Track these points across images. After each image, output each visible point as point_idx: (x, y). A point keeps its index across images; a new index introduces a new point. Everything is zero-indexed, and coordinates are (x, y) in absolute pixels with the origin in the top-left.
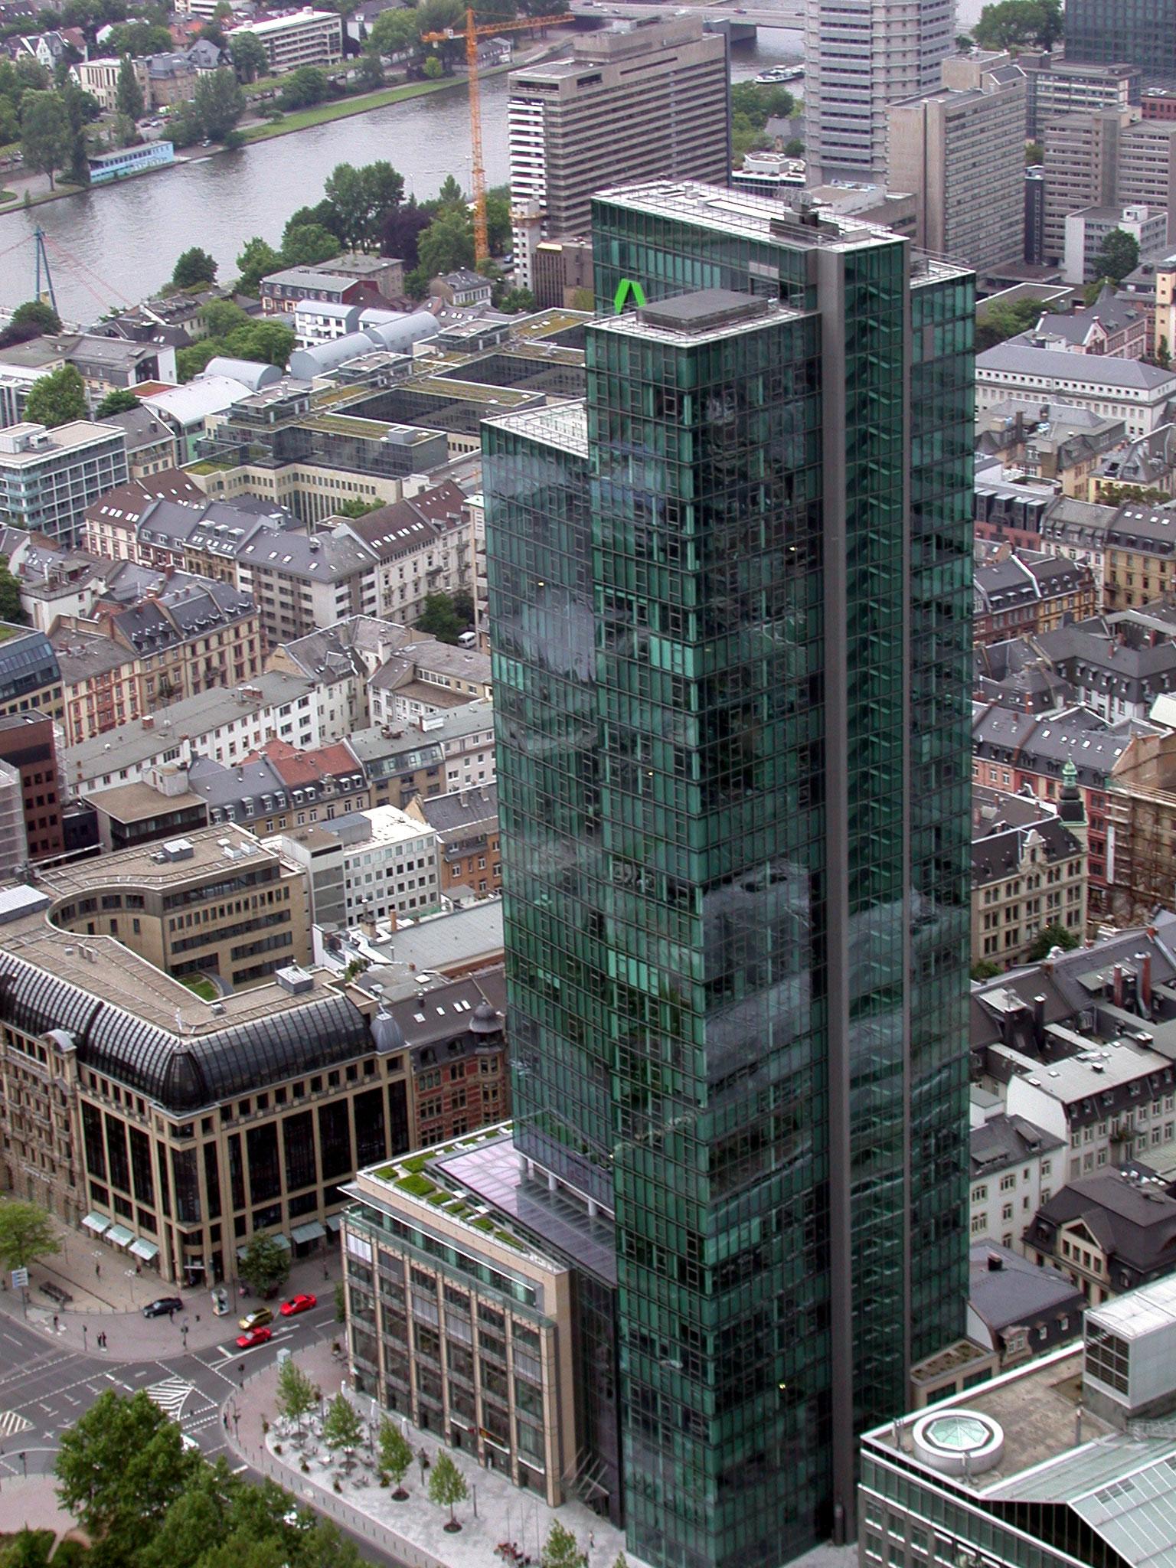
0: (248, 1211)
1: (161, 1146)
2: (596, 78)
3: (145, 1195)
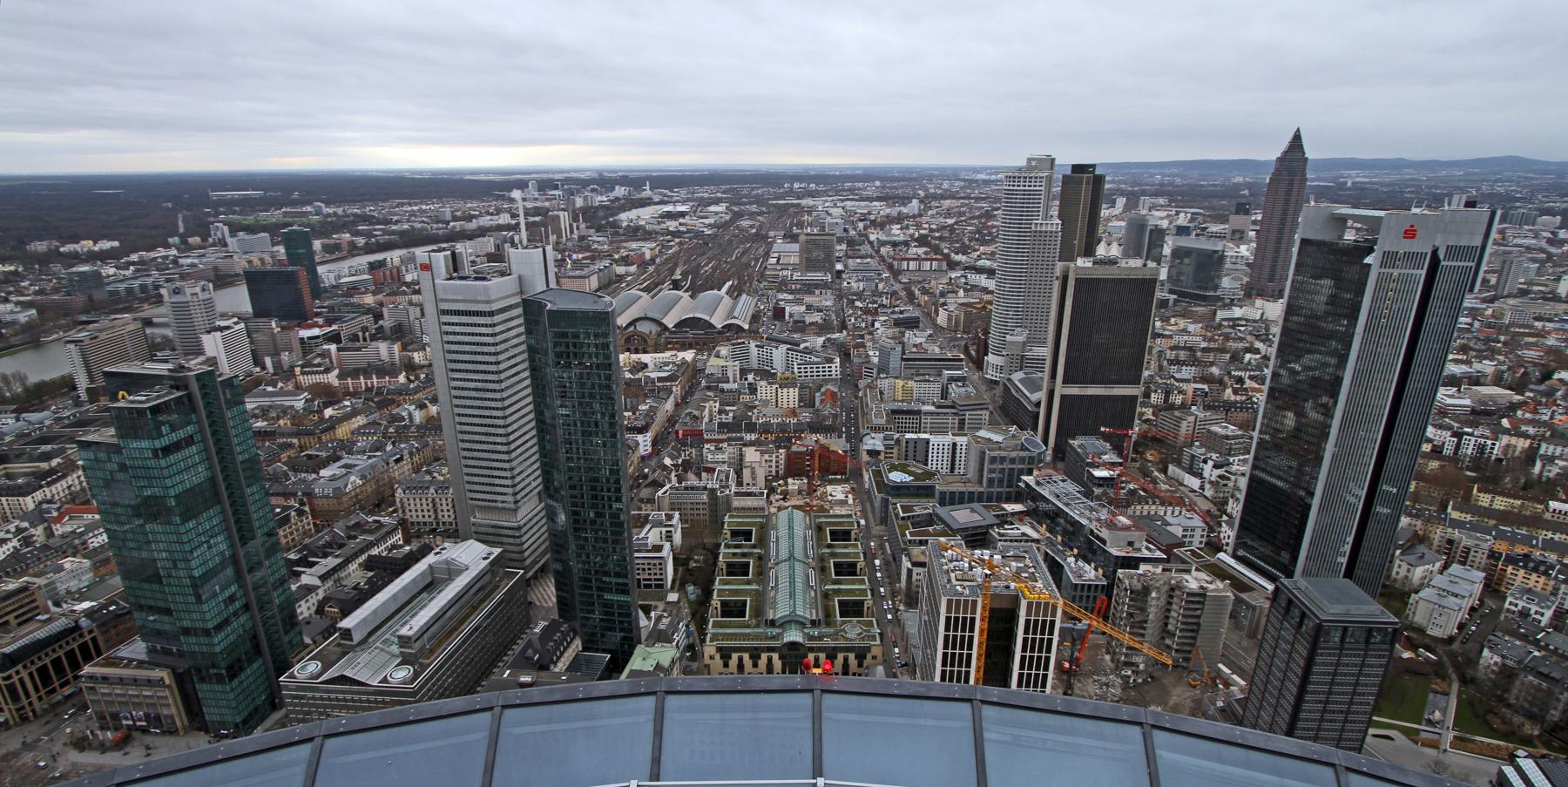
0: (42, 692)
2: (96, 338)
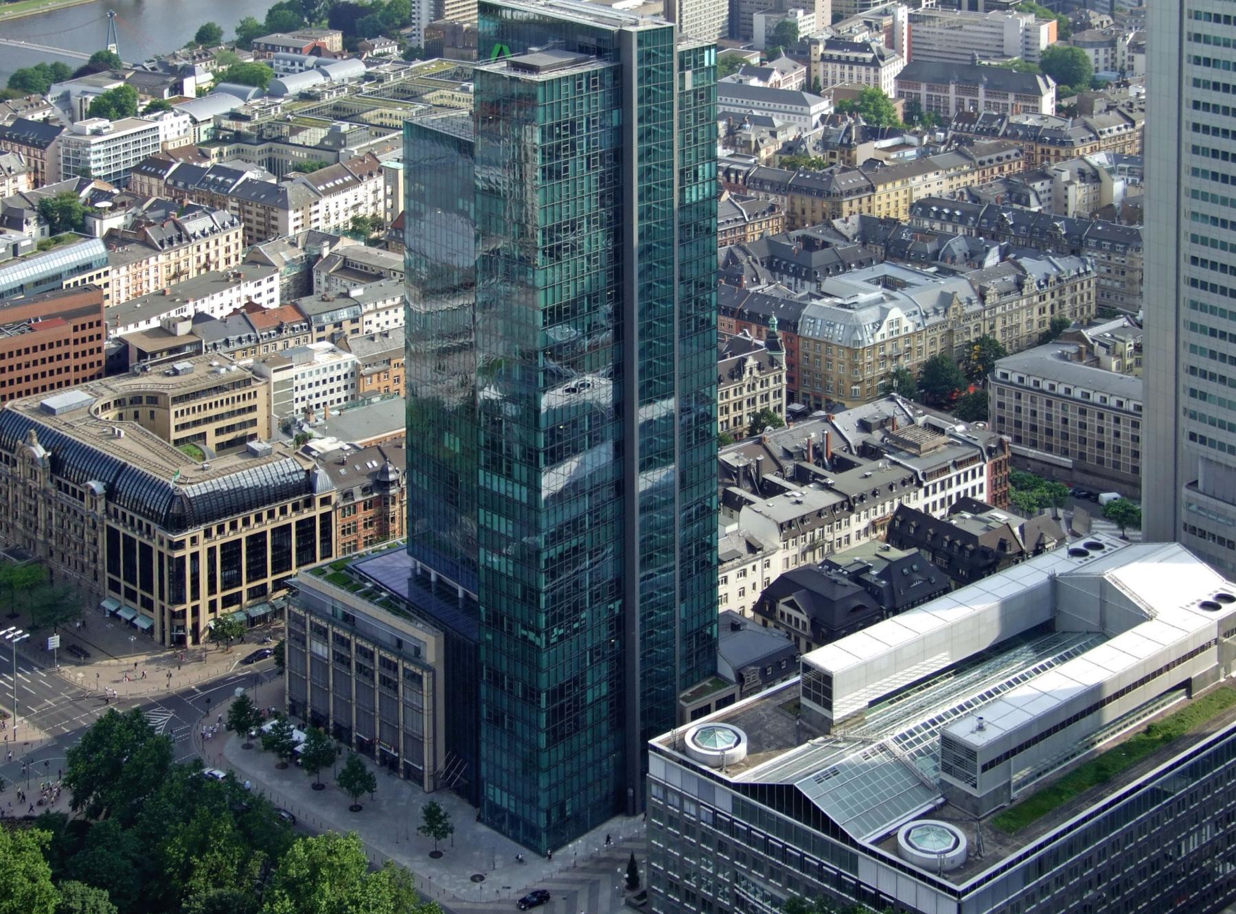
0: (219, 596)
1: (161, 555)
3: (147, 586)
